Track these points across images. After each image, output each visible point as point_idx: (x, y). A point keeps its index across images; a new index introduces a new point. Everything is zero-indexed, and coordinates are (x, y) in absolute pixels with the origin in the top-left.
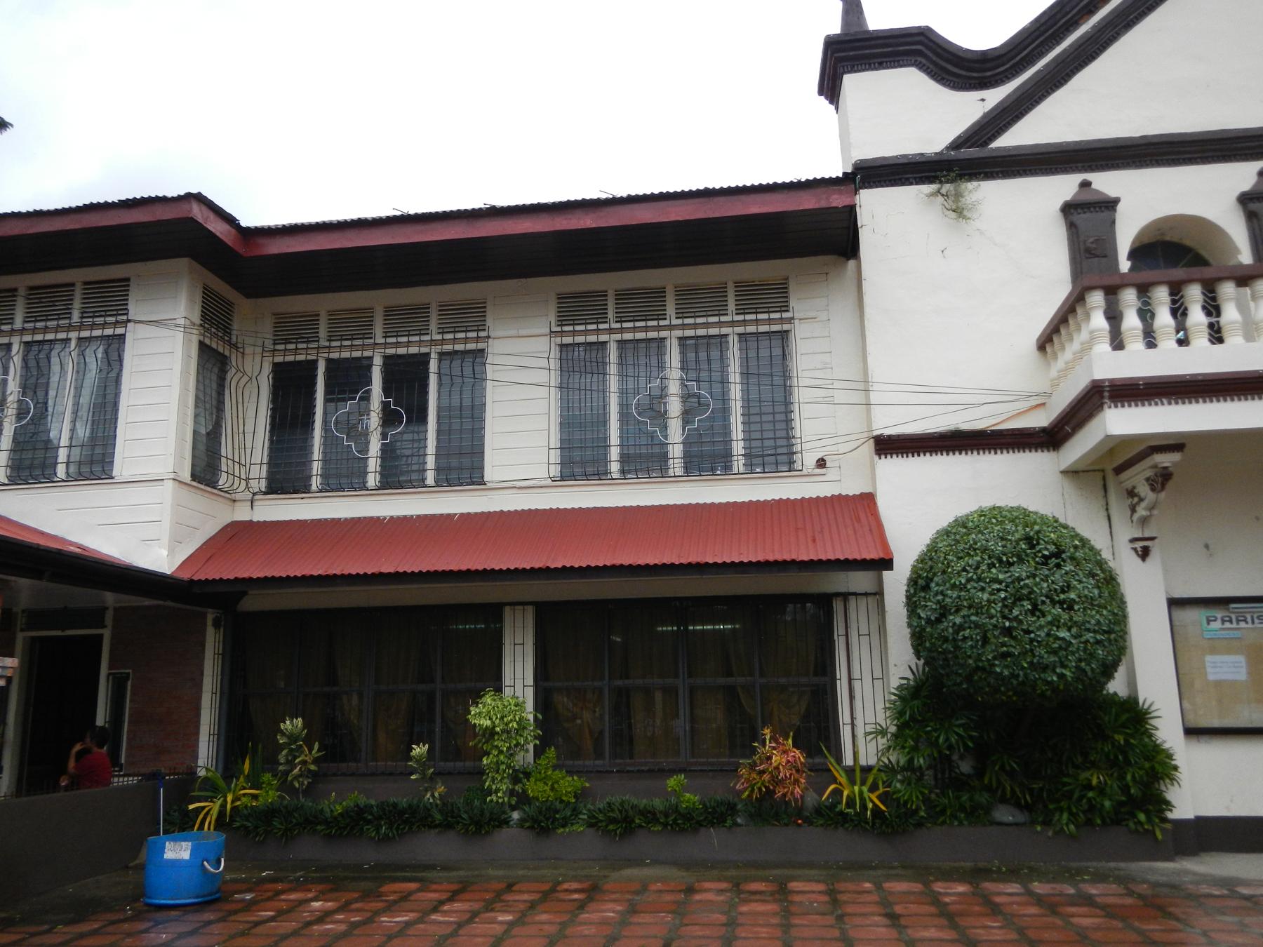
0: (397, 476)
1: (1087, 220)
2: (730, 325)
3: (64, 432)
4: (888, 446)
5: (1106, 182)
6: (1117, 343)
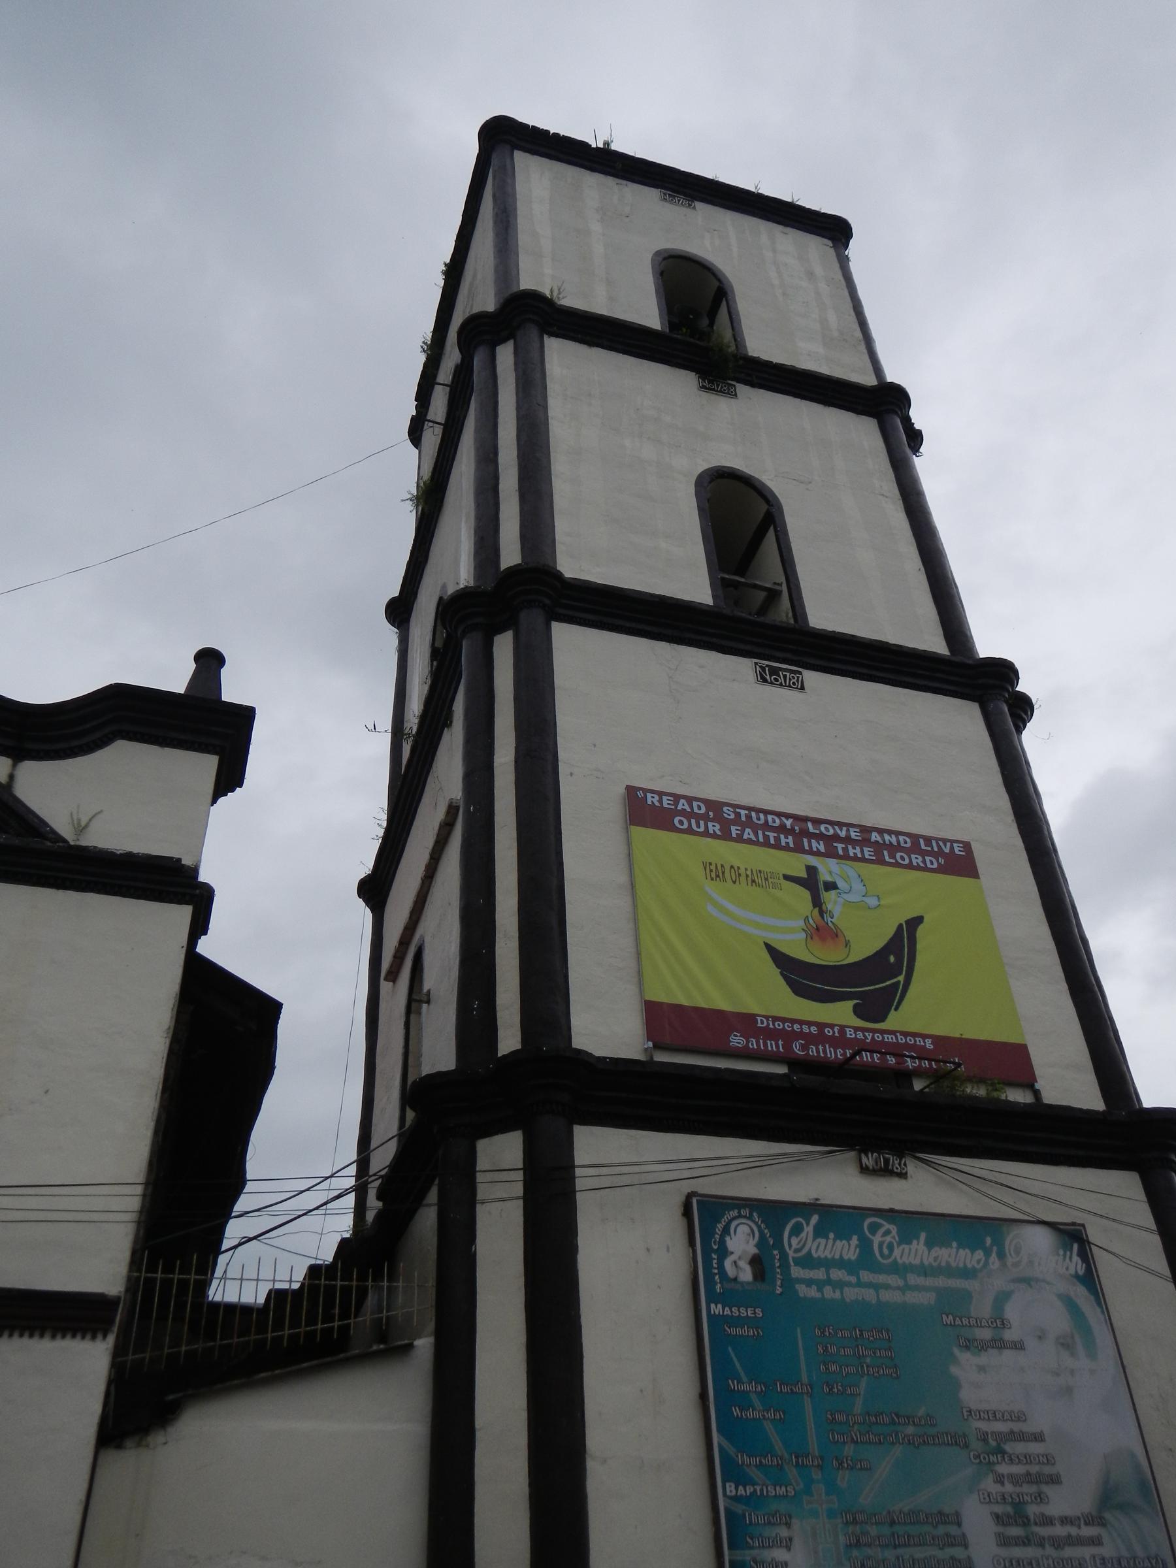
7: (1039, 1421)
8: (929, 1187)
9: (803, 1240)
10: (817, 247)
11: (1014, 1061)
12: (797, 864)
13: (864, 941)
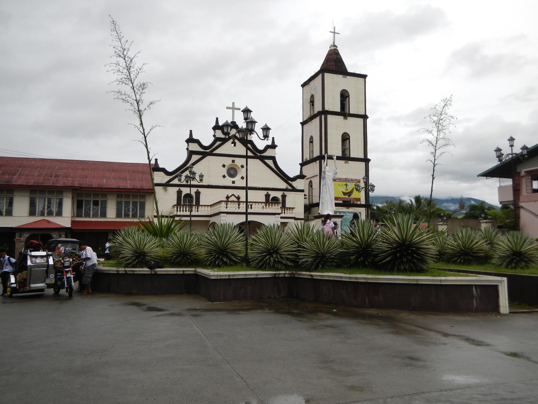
0: (95, 216)
1: (179, 193)
2: (138, 200)
3: (54, 209)
5: (182, 189)
6: (177, 211)
10: (362, 80)
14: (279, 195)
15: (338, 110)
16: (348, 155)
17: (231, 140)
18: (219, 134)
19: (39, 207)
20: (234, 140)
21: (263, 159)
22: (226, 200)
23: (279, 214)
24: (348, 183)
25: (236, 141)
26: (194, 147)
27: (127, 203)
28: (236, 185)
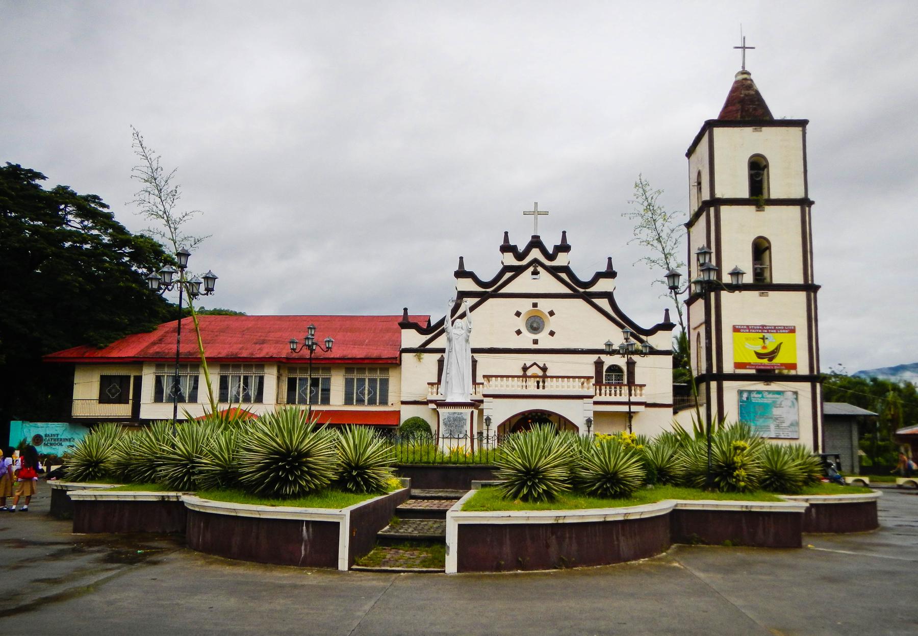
2: (378, 376)
4: (403, 403)
7: (784, 416)
8: (775, 386)
9: (754, 395)
10: (797, 131)
11: (794, 366)
12: (761, 335)
13: (771, 347)
14: (620, 361)
15: (745, 194)
16: (768, 280)
17: (531, 269)
18: (510, 259)
19: (232, 391)
20: (535, 267)
21: (588, 298)
22: (521, 373)
23: (591, 397)
24: (767, 335)
25: (539, 269)
26: (468, 285)
27: (361, 382)
28: (539, 346)
